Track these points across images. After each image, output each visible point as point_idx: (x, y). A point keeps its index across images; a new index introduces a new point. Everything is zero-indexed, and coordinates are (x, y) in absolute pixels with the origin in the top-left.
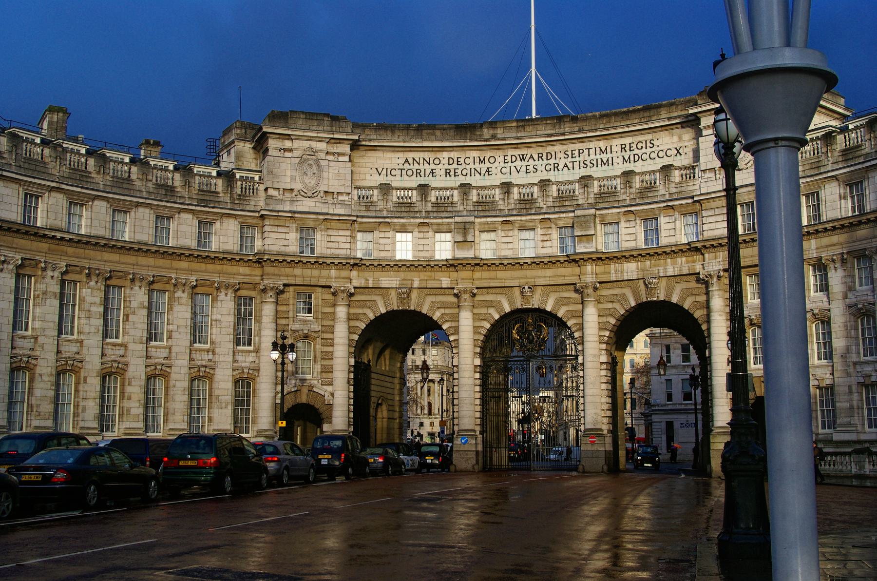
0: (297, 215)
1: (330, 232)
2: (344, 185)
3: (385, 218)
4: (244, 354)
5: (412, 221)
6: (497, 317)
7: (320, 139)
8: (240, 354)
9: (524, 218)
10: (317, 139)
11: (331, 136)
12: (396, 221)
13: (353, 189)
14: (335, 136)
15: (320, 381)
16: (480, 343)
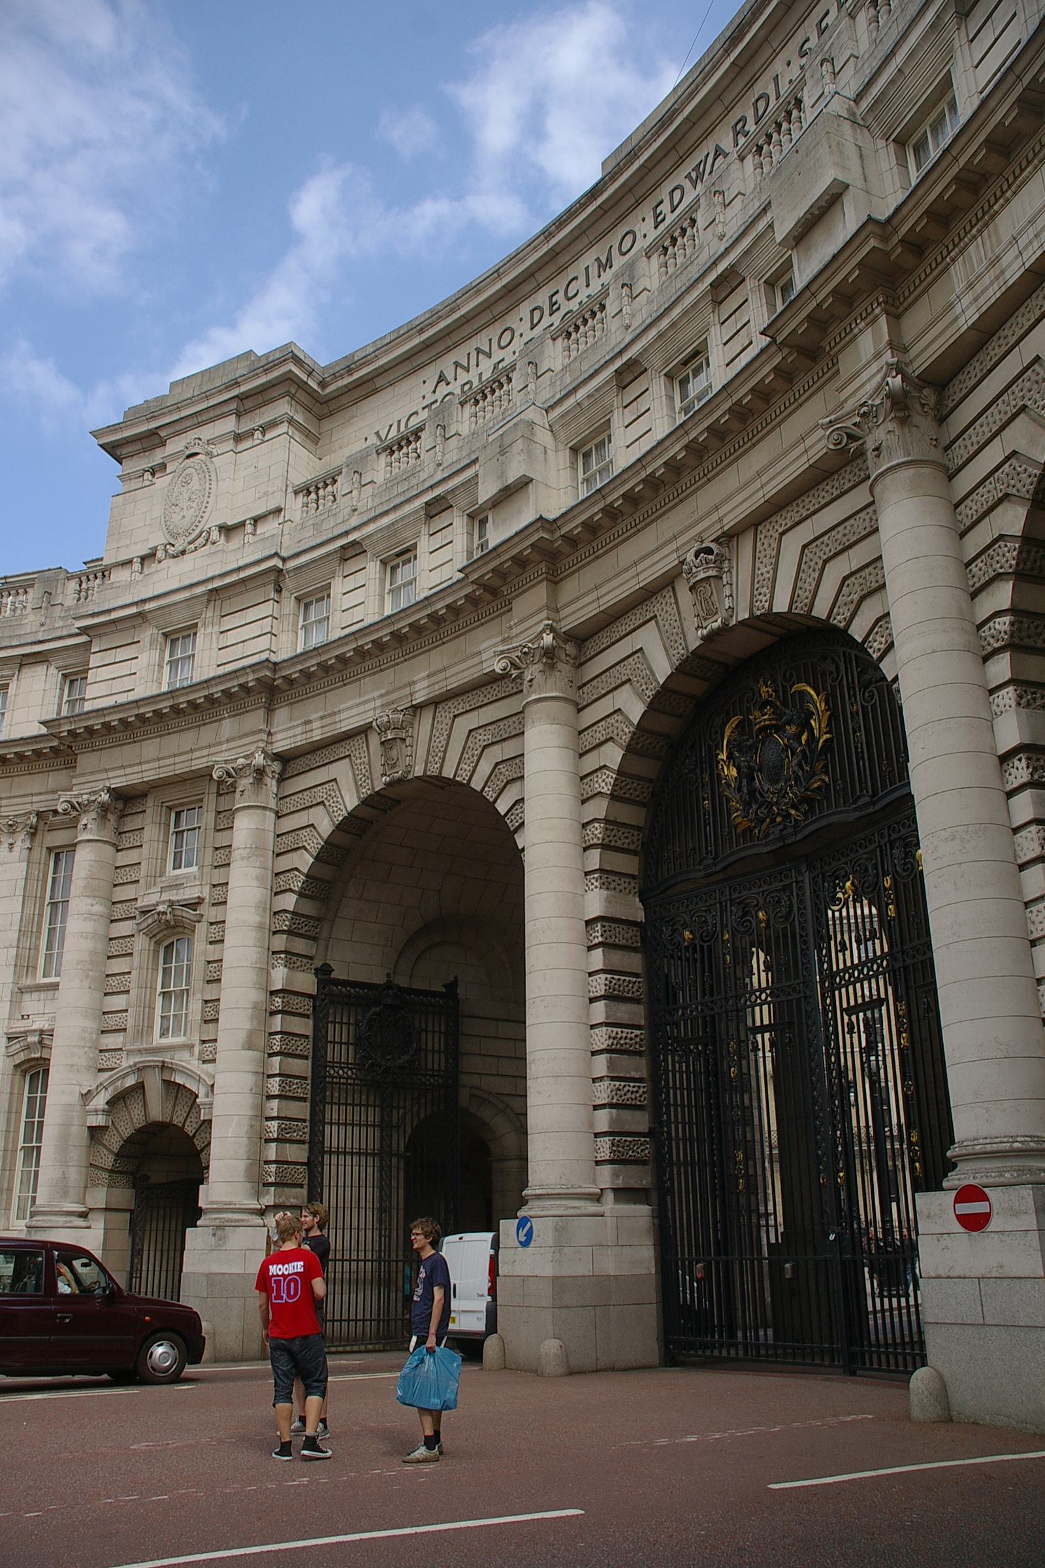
0: (148, 606)
1: (229, 622)
2: (266, 493)
3: (347, 533)
4: (42, 995)
5: (408, 509)
6: (636, 710)
7: (218, 411)
8: (35, 995)
9: (665, 323)
10: (212, 414)
11: (235, 392)
12: (371, 528)
13: (291, 496)
14: (243, 388)
15: (196, 1050)
16: (597, 830)
